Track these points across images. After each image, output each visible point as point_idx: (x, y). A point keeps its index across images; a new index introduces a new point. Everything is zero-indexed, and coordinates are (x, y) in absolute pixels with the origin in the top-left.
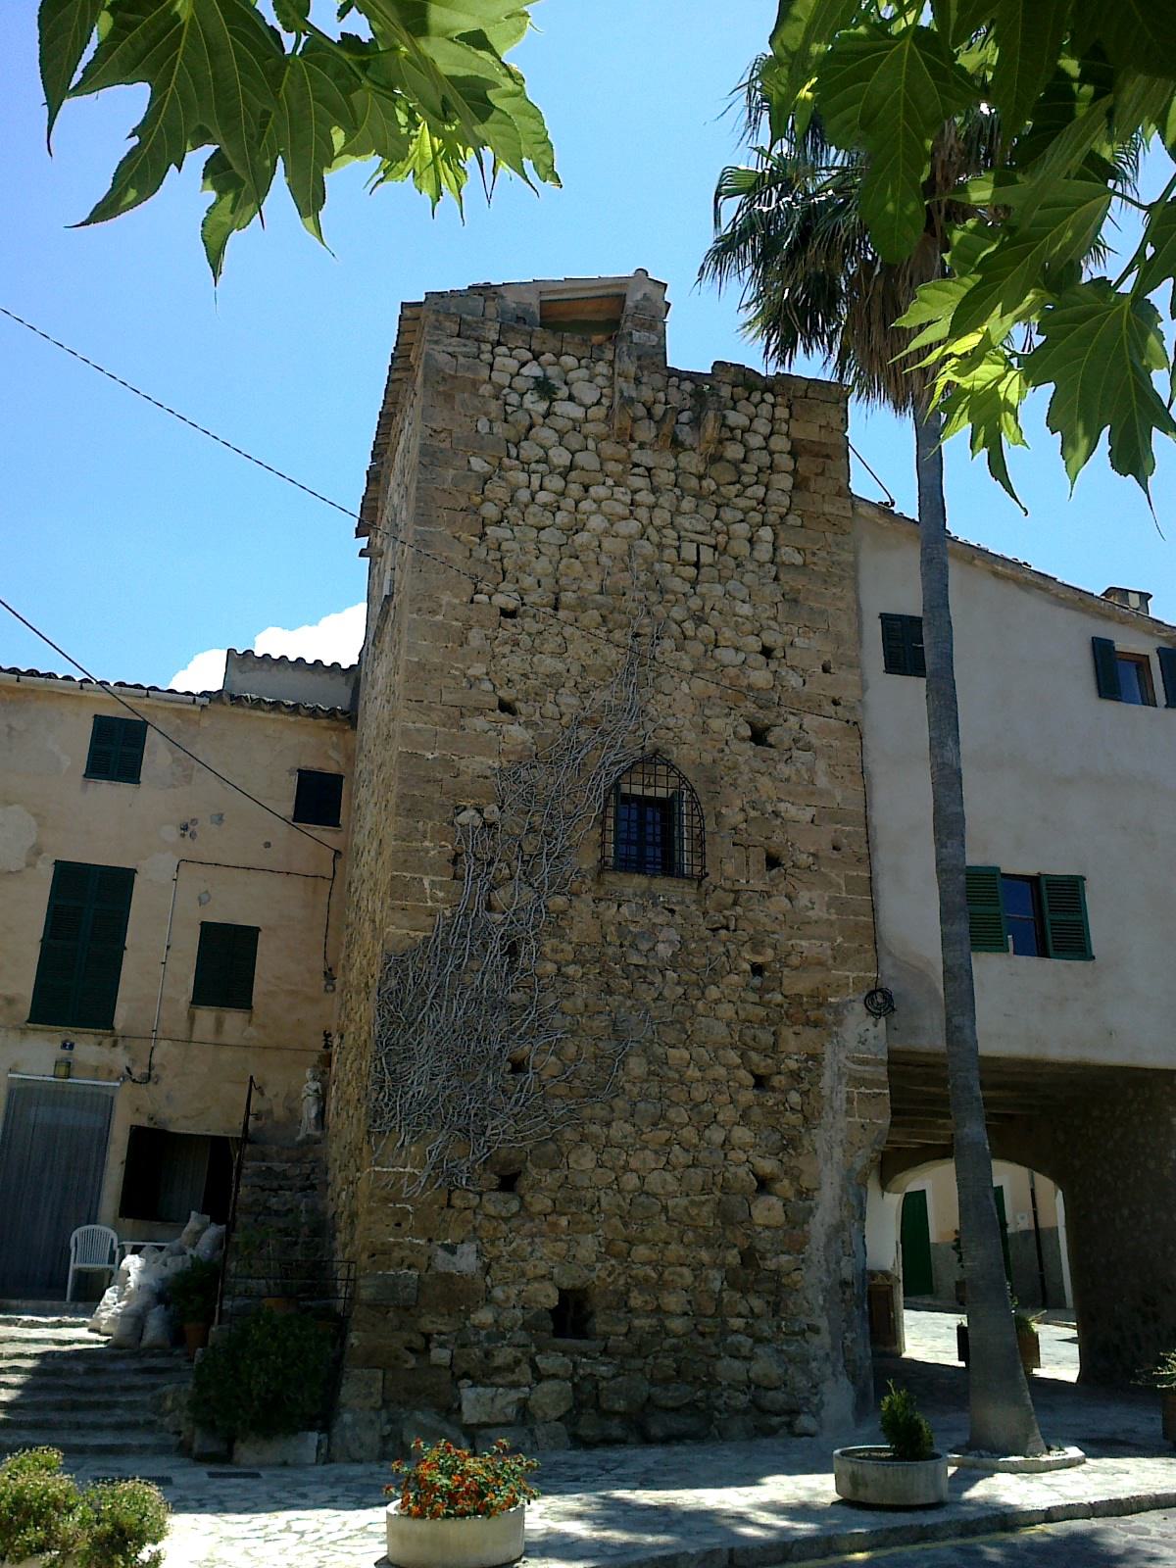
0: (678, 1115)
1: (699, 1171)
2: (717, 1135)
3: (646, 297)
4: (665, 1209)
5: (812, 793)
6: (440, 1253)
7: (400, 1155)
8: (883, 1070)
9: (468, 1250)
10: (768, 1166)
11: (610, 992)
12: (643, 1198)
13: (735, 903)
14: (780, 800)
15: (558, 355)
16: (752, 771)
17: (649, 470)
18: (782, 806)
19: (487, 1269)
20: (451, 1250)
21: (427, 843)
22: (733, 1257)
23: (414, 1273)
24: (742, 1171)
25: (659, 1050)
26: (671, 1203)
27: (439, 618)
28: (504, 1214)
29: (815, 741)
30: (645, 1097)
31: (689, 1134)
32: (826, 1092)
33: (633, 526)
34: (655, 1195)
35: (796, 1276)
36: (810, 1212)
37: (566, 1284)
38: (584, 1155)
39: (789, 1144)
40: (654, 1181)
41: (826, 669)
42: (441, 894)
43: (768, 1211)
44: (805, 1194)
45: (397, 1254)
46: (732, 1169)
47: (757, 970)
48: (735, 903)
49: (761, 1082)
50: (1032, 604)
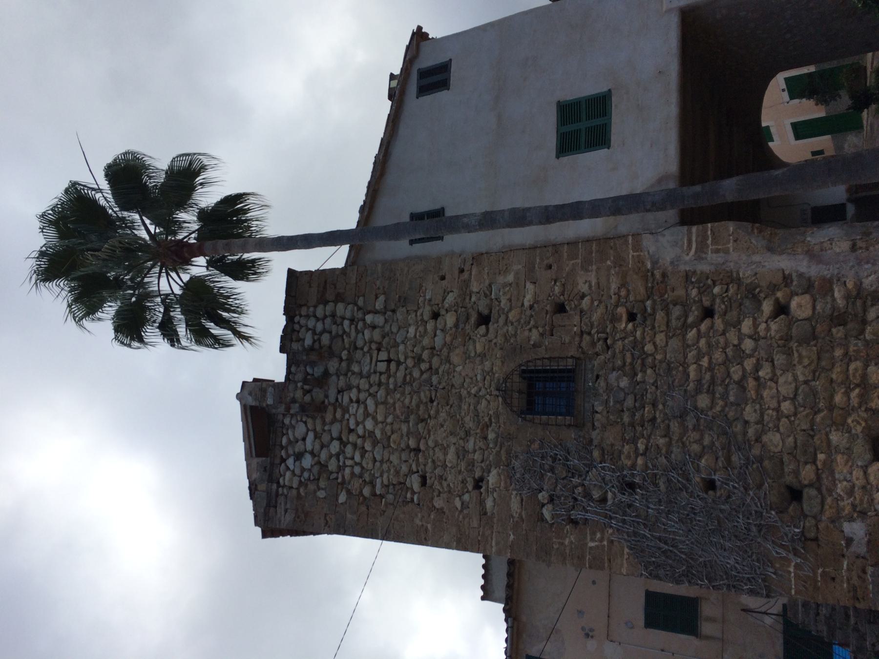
0: (736, 373)
1: (776, 358)
2: (748, 344)
3: (250, 394)
4: (806, 382)
5: (517, 284)
6: (853, 549)
7: (781, 576)
8: (694, 229)
9: (849, 528)
10: (767, 307)
11: (653, 420)
12: (800, 398)
13: (589, 334)
14: (523, 305)
15: (282, 447)
16: (506, 323)
17: (339, 392)
18: (526, 304)
19: (863, 514)
20: (849, 541)
21: (567, 542)
22: (838, 332)
23: (870, 570)
24: (774, 326)
25: (691, 386)
26: (801, 378)
27: (429, 526)
28: (819, 500)
29: (487, 282)
30: (725, 396)
31: (749, 364)
32: (713, 268)
33: (370, 403)
34: (797, 389)
35: (850, 285)
36: (801, 275)
37: (868, 456)
38: (771, 441)
39: (753, 294)
40: (786, 390)
41: (443, 278)
42: (598, 535)
43: (801, 306)
44: (787, 279)
45: (855, 581)
46: (773, 333)
47: (632, 317)
48: (589, 334)
49: (708, 313)
50: (397, 150)
